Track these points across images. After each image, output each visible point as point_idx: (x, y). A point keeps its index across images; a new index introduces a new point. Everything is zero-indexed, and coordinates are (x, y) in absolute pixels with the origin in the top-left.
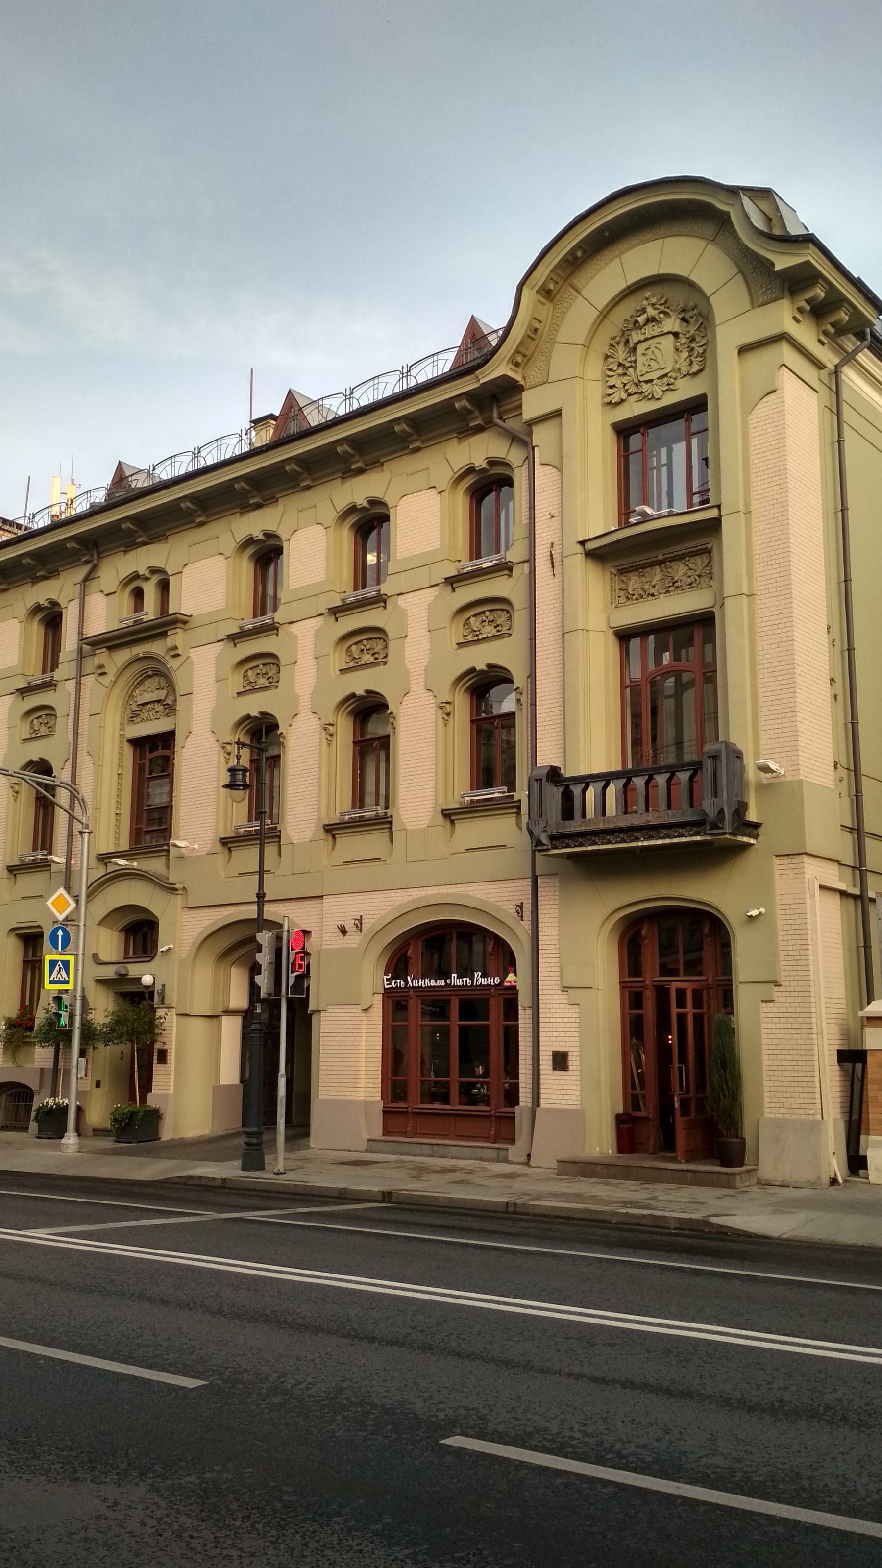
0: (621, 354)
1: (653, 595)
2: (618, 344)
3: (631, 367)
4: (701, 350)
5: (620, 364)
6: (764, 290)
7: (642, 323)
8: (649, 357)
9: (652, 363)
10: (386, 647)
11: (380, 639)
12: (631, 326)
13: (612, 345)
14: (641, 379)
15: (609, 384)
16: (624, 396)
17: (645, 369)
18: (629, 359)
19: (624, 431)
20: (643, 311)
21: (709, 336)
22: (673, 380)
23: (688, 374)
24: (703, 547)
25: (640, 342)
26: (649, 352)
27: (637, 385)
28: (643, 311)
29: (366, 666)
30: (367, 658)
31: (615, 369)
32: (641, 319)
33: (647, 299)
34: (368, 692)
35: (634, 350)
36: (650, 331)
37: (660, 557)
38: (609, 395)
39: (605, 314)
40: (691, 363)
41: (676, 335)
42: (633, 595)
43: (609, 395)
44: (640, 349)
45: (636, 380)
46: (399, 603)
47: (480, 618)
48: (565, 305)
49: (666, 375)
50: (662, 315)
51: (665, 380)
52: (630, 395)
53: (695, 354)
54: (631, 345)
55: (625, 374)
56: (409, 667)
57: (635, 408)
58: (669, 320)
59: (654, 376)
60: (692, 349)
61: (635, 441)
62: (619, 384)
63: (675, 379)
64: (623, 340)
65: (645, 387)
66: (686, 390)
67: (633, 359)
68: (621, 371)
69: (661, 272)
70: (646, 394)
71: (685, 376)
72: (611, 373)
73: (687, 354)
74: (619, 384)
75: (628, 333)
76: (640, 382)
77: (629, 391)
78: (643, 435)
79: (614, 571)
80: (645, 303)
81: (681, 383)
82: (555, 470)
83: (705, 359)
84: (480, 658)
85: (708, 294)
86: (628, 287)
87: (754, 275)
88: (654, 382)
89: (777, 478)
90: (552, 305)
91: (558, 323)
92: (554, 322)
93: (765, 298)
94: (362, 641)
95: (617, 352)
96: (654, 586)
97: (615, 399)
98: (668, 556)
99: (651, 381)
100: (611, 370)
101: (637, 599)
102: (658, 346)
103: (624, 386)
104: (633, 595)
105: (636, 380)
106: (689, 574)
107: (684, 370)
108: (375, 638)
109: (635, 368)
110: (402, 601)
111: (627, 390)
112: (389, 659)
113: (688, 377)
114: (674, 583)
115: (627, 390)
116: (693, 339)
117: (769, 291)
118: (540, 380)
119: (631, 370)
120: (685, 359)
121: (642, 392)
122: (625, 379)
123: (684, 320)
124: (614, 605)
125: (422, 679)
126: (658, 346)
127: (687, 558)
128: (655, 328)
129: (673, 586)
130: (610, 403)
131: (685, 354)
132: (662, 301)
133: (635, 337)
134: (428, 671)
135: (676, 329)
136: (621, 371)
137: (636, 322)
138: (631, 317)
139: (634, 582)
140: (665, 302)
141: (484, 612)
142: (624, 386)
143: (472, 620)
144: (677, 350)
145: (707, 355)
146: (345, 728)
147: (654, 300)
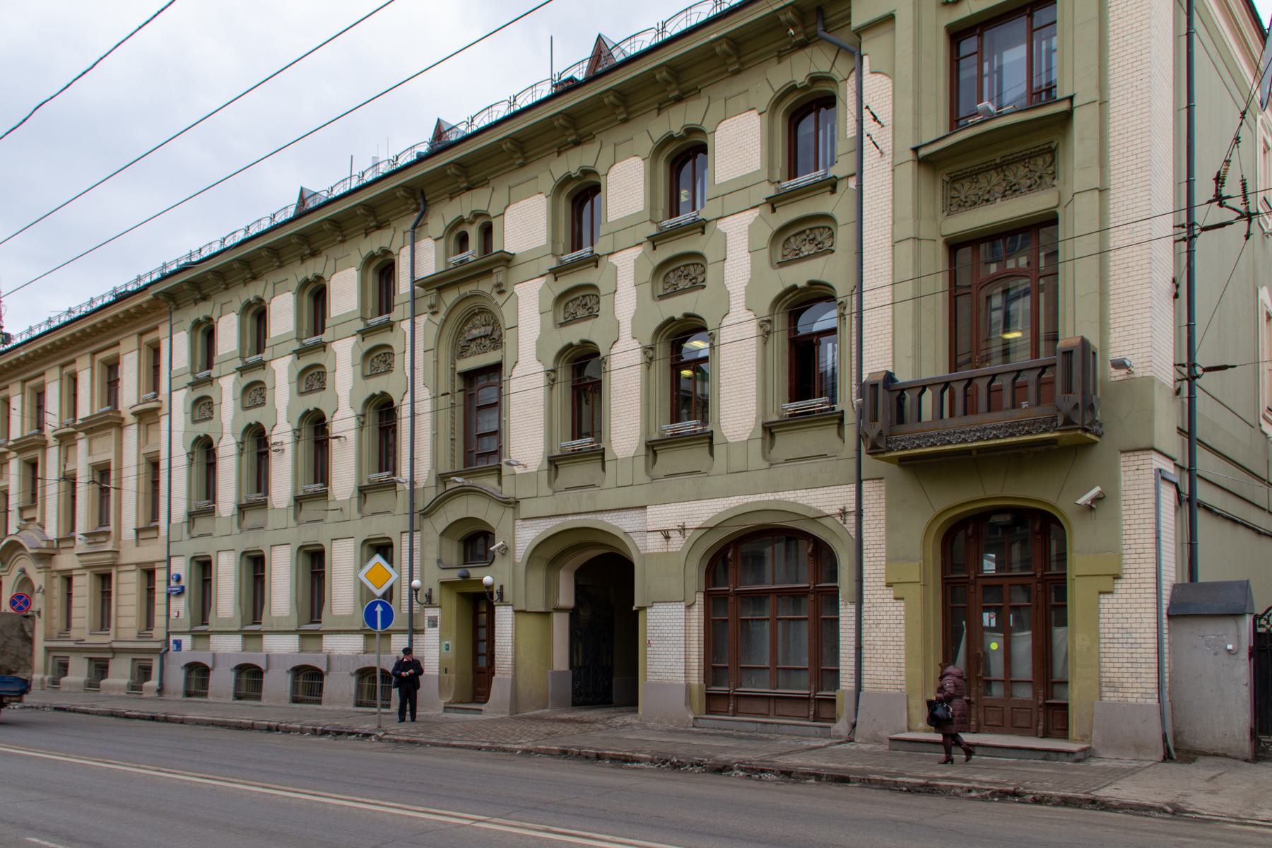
10: (704, 272)
34: (687, 316)
47: (800, 238)
84: (800, 275)
112: (708, 283)
134: (748, 290)
141: (804, 232)
143: (792, 240)
146: (662, 352)
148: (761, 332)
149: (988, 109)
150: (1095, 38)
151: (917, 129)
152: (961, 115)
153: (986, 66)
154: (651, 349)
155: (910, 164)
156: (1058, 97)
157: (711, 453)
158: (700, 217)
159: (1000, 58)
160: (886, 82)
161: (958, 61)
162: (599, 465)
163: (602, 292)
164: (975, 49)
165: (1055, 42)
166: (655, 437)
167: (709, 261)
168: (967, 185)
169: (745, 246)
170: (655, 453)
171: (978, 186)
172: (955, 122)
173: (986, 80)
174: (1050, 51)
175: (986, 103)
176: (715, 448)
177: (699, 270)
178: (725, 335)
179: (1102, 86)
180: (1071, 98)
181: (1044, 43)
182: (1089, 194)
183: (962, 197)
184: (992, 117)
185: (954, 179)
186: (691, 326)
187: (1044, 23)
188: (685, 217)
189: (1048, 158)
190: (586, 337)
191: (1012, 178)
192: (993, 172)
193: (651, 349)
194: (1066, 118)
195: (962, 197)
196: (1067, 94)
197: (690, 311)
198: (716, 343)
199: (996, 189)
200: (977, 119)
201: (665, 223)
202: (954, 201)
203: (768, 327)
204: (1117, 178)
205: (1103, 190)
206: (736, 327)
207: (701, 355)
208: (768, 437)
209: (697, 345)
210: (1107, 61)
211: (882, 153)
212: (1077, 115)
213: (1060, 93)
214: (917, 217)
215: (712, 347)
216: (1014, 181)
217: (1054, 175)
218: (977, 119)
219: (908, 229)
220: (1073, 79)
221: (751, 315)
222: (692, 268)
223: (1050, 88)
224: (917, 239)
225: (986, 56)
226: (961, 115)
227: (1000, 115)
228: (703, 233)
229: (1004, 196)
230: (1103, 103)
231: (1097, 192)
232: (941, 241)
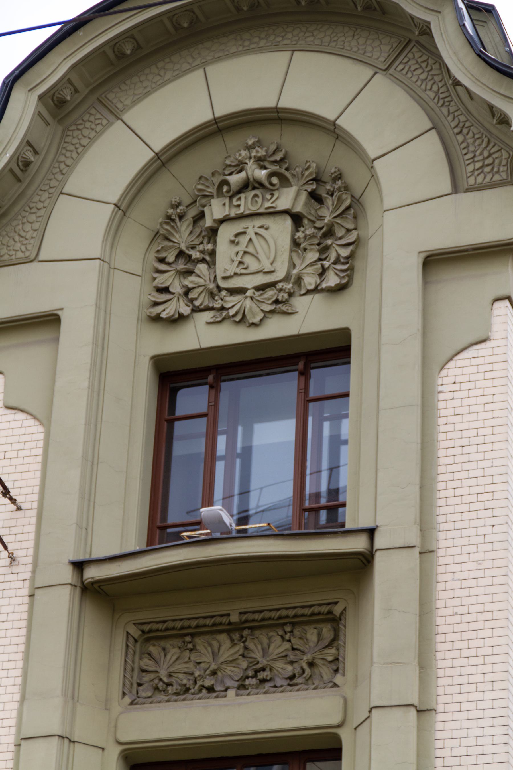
0: (183, 236)
1: (211, 689)
2: (181, 217)
3: (203, 260)
4: (345, 252)
5: (181, 254)
6: (478, 165)
7: (234, 187)
8: (241, 248)
9: (248, 259)
12: (213, 190)
13: (169, 218)
14: (223, 284)
15: (155, 283)
16: (186, 310)
17: (233, 269)
18: (201, 247)
19: (172, 376)
20: (240, 167)
21: (362, 233)
22: (286, 296)
23: (316, 290)
24: (325, 609)
25: (222, 221)
26: (243, 240)
27: (212, 295)
28: (240, 167)
31: (171, 258)
32: (235, 179)
33: (249, 148)
35: (213, 232)
36: (246, 203)
37: (234, 618)
38: (156, 304)
39: (164, 161)
40: (324, 271)
41: (297, 219)
42: (168, 684)
43: (156, 304)
44: (226, 233)
45: (212, 286)
48: (86, 132)
49: (272, 285)
50: (275, 180)
51: (270, 293)
52: (196, 310)
53: (333, 257)
54: (208, 222)
55: (190, 273)
57: (202, 335)
58: (285, 190)
59: (248, 282)
60: (327, 248)
61: (192, 399)
62: (177, 288)
63: (291, 295)
64: (193, 212)
65: (231, 301)
66: (311, 317)
67: (210, 247)
68: (181, 266)
69: (285, 103)
70: (232, 312)
71: (308, 292)
72: (163, 267)
73: (316, 256)
74: (177, 288)
75: (204, 201)
76: (219, 289)
77: (197, 303)
78: (211, 387)
79: (135, 632)
80: (244, 153)
81: (300, 303)
82: (32, 422)
83: (351, 269)
85: (372, 154)
86: (216, 121)
87: (460, 138)
88: (249, 293)
89: (488, 496)
90: (60, 128)
91: (69, 162)
92: (62, 158)
93: (480, 179)
95: (178, 231)
96: (214, 673)
97: (168, 311)
98: (250, 617)
99: (241, 291)
100: (162, 260)
101: (177, 694)
102: (262, 231)
103: (186, 294)
104: (168, 684)
105: (212, 286)
106: (292, 658)
107: (310, 281)
109: (211, 264)
111: (192, 301)
113: (317, 297)
114: (256, 672)
115: (192, 301)
116: (329, 233)
117: (487, 169)
118: (20, 255)
119: (202, 268)
120: (311, 264)
121: (223, 308)
122: (190, 281)
123: (315, 197)
124: (127, 700)
126: (262, 231)
127: (288, 628)
128: (260, 200)
129: (257, 679)
130: (157, 319)
131: (313, 256)
132: (278, 157)
133: (217, 209)
135: (299, 208)
136: (181, 266)
137: (225, 182)
138: (213, 174)
139: (171, 660)
140: (282, 160)
142: (186, 294)
144: (296, 244)
145: (358, 264)
147: (262, 153)
149: (221, 521)
150: (415, 437)
151: (85, 529)
152: (172, 519)
153: (222, 442)
155: (67, 590)
156: (349, 526)
159: (248, 434)
160: (34, 430)
161: (171, 422)
164: (203, 408)
165: (346, 428)
168: (173, 652)
171: (194, 657)
172: (160, 531)
173: (220, 467)
174: (337, 442)
175: (217, 509)
179: (426, 523)
180: (371, 532)
181: (326, 425)
182: (398, 713)
183: (163, 674)
184: (226, 537)
185: (150, 636)
187: (328, 392)
189: (327, 632)
191: (258, 655)
192: (223, 637)
194: (360, 566)
195: (163, 674)
196: (365, 523)
199: (229, 670)
200: (201, 533)
202: (147, 678)
204: (447, 695)
205: (424, 711)
210: (434, 480)
211: (12, 558)
212: (381, 563)
213: (354, 517)
214: (72, 696)
216: (263, 662)
217: (336, 665)
218: (201, 533)
219: (50, 717)
220: (376, 500)
223: (335, 505)
224: (67, 739)
225: (221, 427)
226: (172, 519)
227: (243, 535)
229: (242, 687)
230: (427, 552)
231: (413, 712)
232: (114, 753)
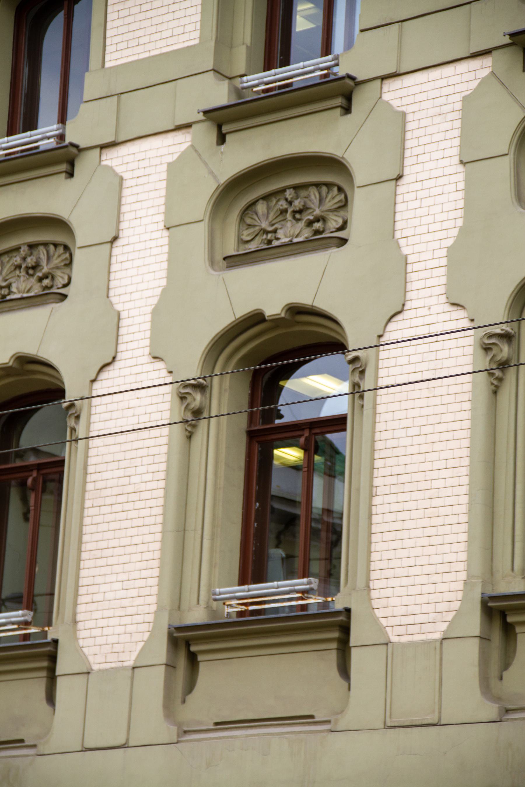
10: (344, 205)
11: (329, 185)
29: (292, 249)
30: (290, 231)
34: (296, 311)
46: (386, 97)
56: (405, 251)
94: (283, 191)
108: (317, 185)
110: (394, 93)
112: (353, 233)
125: (440, 277)
134: (456, 257)
146: (227, 397)
148: (484, 363)
154: (200, 387)
157: (344, 670)
158: (341, 71)
162: (37, 687)
163: (82, 237)
166: (197, 616)
167: (359, 180)
169: (452, 149)
170: (193, 660)
176: (355, 654)
177: (333, 199)
178: (391, 365)
186: (303, 338)
188: (303, 69)
190: (30, 349)
193: (200, 387)
197: (305, 299)
198: (367, 384)
201: (252, 79)
203: (505, 351)
206: (422, 346)
207: (328, 410)
208: (497, 636)
209: (318, 387)
215: (357, 392)
221: (459, 319)
222: (313, 193)
228: (347, 110)
